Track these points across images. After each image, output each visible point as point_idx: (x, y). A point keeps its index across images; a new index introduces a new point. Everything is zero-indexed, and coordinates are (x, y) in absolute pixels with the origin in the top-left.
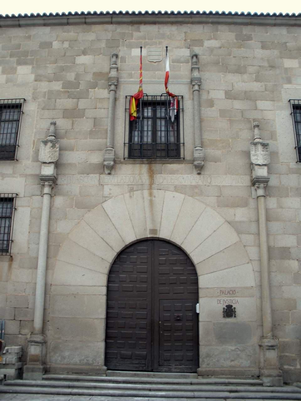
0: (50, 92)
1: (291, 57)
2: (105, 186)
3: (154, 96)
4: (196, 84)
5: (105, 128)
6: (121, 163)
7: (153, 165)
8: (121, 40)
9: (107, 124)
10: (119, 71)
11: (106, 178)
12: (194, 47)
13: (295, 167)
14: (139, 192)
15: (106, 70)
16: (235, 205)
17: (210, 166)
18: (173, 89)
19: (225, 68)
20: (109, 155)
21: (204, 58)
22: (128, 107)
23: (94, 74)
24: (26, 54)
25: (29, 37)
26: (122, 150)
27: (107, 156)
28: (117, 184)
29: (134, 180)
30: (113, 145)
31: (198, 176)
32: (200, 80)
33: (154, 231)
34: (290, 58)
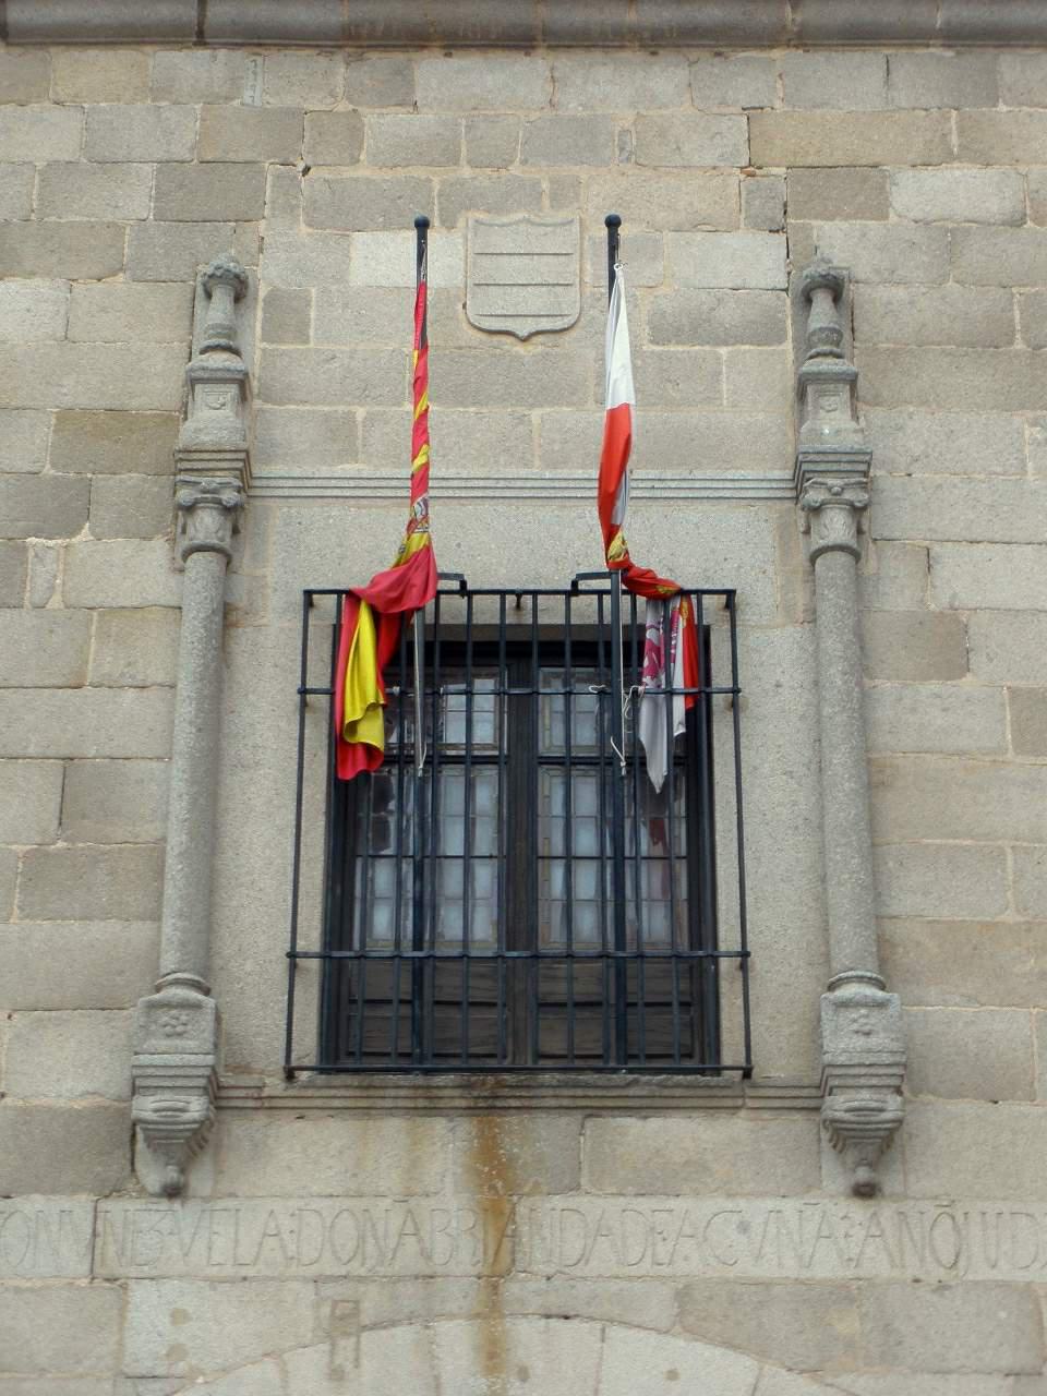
2: (140, 1294)
3: (519, 594)
4: (835, 503)
5: (149, 831)
6: (265, 1104)
7: (513, 1120)
8: (270, 169)
9: (161, 799)
10: (257, 404)
11: (145, 1225)
12: (815, 223)
14: (403, 1334)
15: (157, 387)
17: (950, 1129)
18: (666, 542)
20: (178, 1042)
21: (893, 302)
22: (319, 678)
23: (65, 416)
26: (272, 1009)
27: (164, 1052)
28: (229, 1270)
29: (362, 1238)
30: (206, 969)
31: (858, 1210)
32: (860, 466)
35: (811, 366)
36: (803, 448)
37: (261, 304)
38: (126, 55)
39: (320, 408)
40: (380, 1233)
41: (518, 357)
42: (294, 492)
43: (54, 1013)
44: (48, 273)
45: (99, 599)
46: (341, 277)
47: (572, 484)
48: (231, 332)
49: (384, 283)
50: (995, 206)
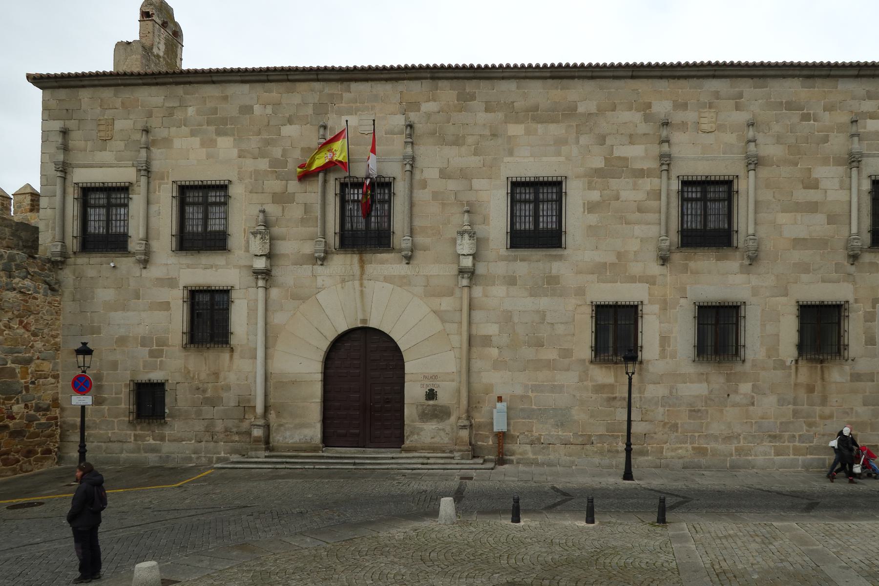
0: (257, 172)
1: (518, 121)
6: (332, 253)
11: (319, 269)
13: (506, 254)
16: (441, 295)
17: (419, 255)
19: (441, 139)
21: (420, 128)
23: (302, 149)
24: (224, 121)
25: (225, 98)
26: (333, 240)
33: (364, 321)
34: (516, 123)
38: (307, 83)
50: (436, 110)
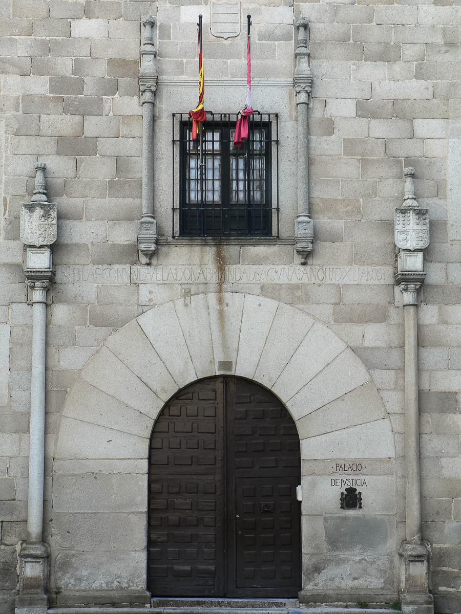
2: (141, 287)
3: (225, 114)
6: (168, 244)
10: (158, 58)
11: (143, 272)
12: (301, 4)
14: (201, 296)
15: (132, 53)
20: (148, 232)
21: (321, 29)
23: (110, 61)
26: (170, 221)
27: (145, 234)
28: (161, 282)
29: (191, 275)
30: (153, 212)
35: (298, 51)
36: (295, 76)
37: (158, 28)
39: (174, 59)
40: (195, 274)
41: (224, 44)
42: (169, 84)
43: (118, 221)
44: (102, 18)
45: (122, 113)
46: (178, 20)
47: (238, 82)
48: (151, 39)
49: (190, 22)
